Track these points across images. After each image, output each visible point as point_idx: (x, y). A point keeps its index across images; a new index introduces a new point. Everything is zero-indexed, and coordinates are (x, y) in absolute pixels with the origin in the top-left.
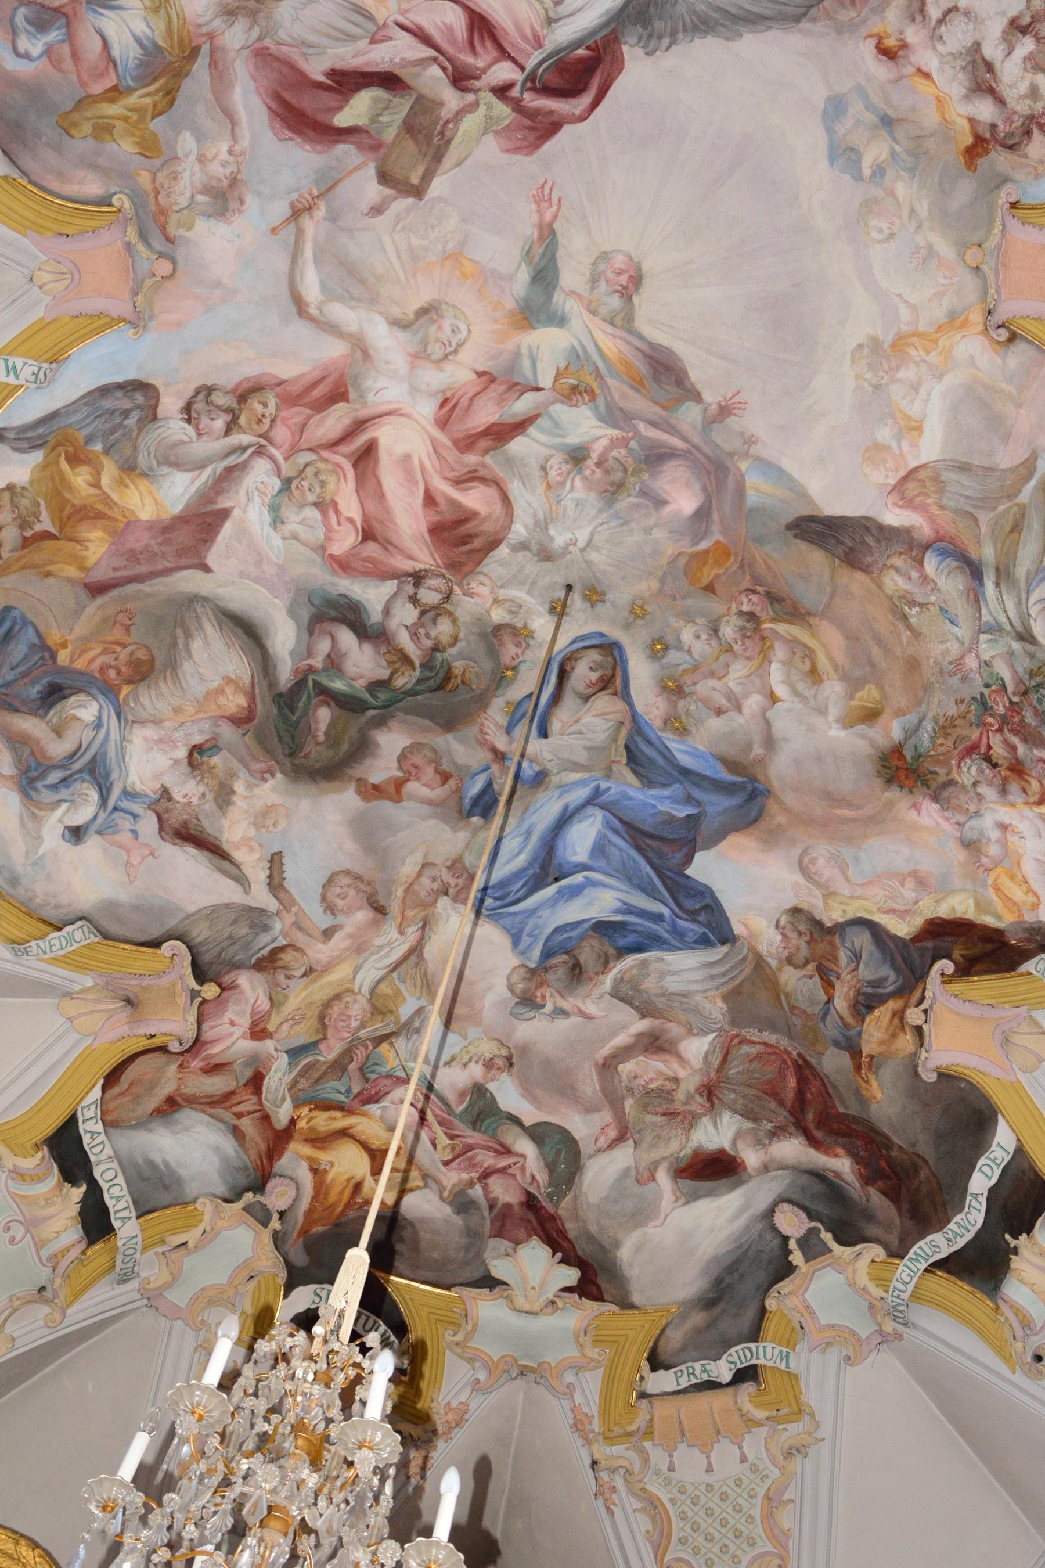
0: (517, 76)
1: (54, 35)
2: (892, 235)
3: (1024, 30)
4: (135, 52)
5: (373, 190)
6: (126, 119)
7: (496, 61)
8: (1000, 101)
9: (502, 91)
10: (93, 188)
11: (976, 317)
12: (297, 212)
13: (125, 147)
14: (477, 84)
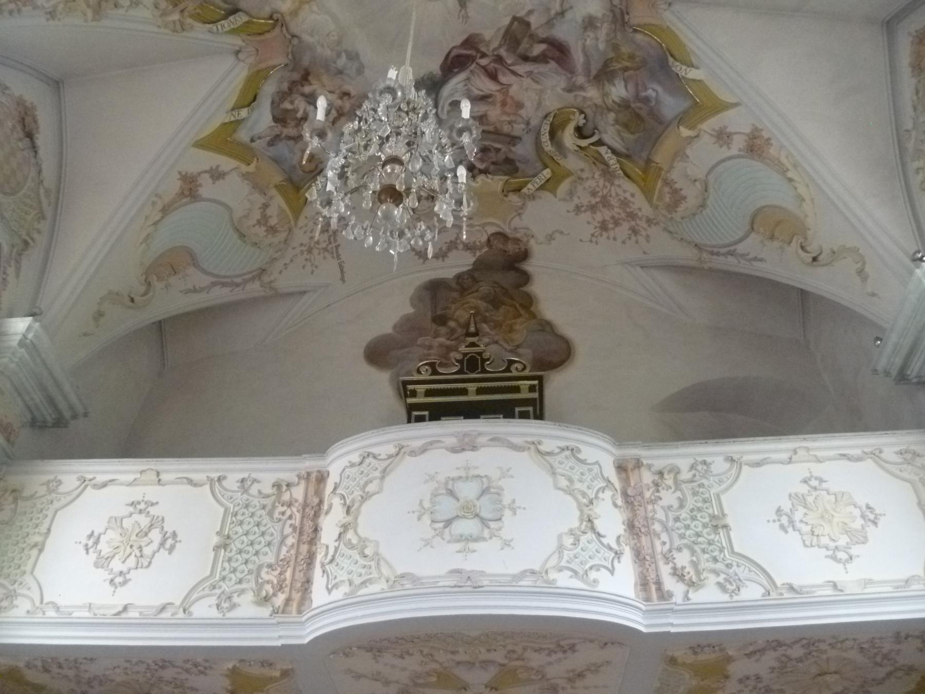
0: (479, 61)
1: (643, 94)
2: (328, 35)
3: (302, 119)
4: (616, 82)
5: (534, 20)
6: (623, 59)
7: (487, 65)
8: (303, 95)
9: (484, 55)
10: (639, 37)
11: (288, 18)
12: (562, 13)
13: (625, 49)
14: (494, 58)
